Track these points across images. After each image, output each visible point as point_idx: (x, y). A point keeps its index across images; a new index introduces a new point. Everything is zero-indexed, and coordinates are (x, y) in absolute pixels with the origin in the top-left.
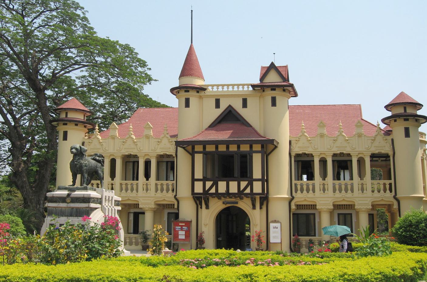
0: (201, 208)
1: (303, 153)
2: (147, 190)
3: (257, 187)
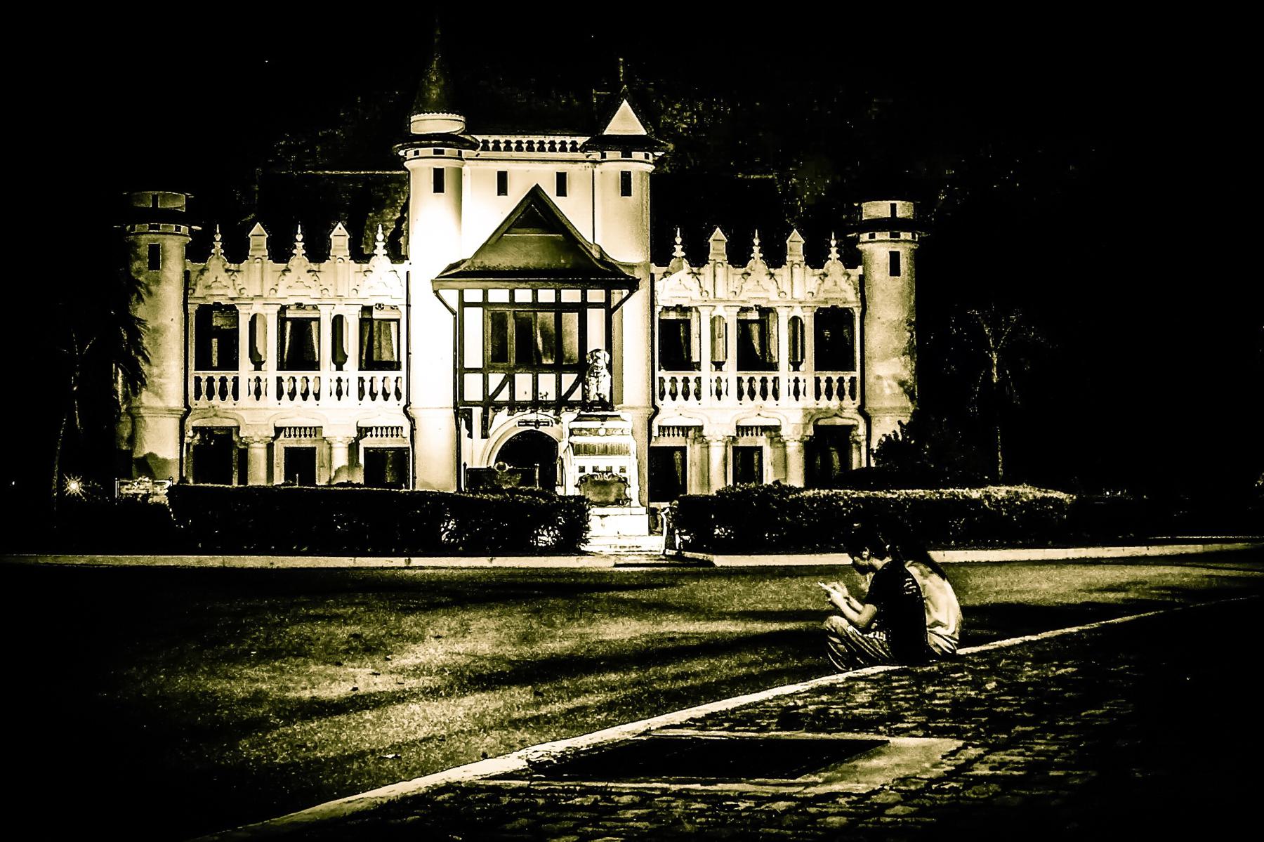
0: (470, 436)
2: (339, 393)
3: (600, 386)
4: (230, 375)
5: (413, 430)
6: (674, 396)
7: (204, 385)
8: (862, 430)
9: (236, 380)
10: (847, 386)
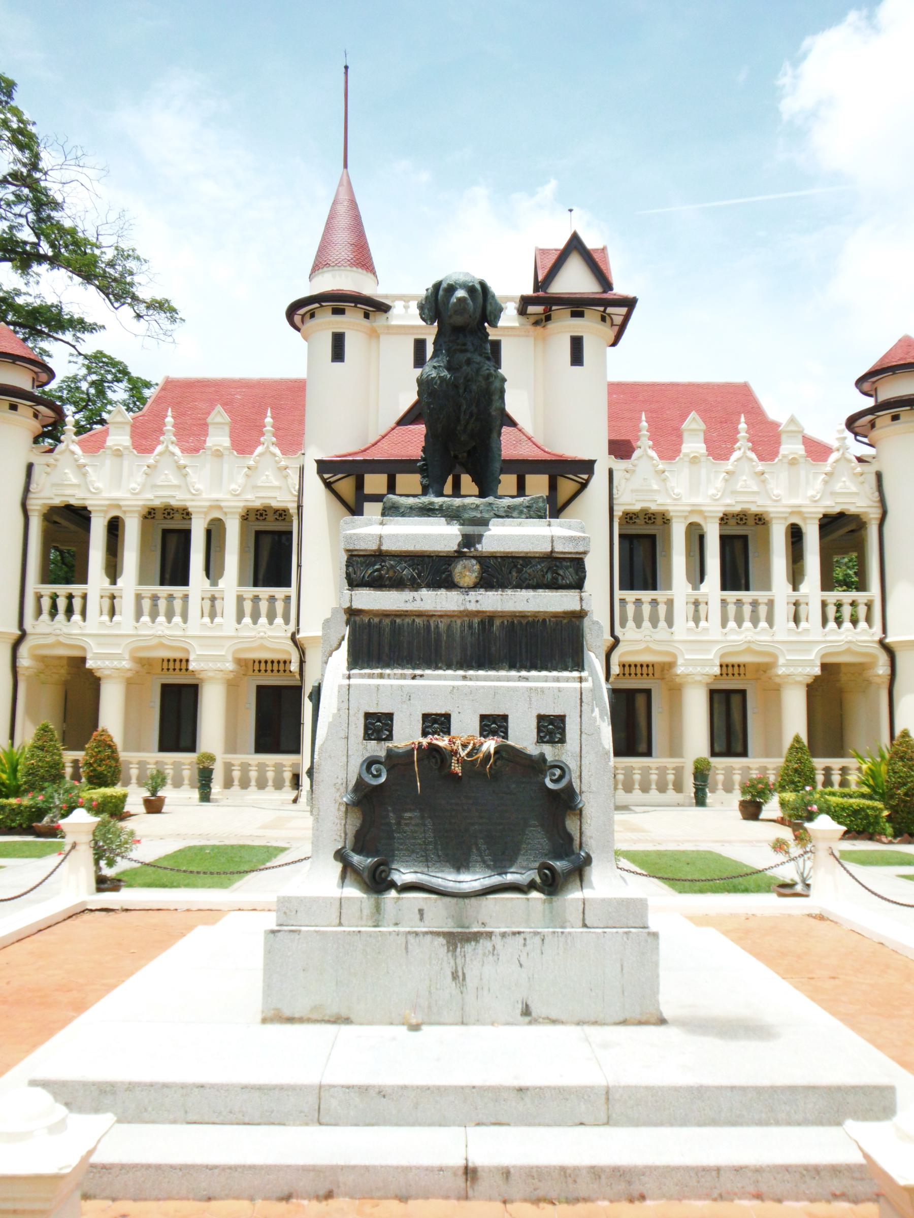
1: (642, 510)
4: (76, 589)
5: (302, 662)
6: (638, 622)
7: (46, 603)
8: (882, 669)
9: (84, 597)
10: (862, 611)
